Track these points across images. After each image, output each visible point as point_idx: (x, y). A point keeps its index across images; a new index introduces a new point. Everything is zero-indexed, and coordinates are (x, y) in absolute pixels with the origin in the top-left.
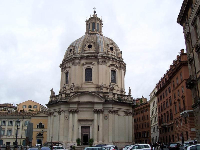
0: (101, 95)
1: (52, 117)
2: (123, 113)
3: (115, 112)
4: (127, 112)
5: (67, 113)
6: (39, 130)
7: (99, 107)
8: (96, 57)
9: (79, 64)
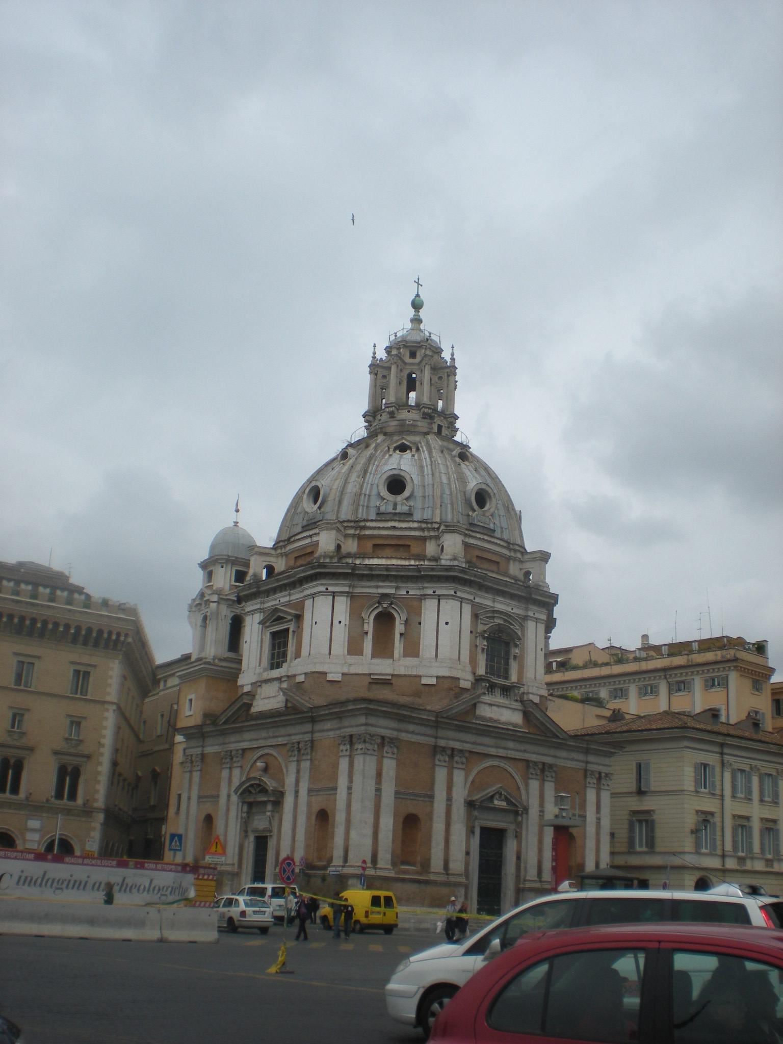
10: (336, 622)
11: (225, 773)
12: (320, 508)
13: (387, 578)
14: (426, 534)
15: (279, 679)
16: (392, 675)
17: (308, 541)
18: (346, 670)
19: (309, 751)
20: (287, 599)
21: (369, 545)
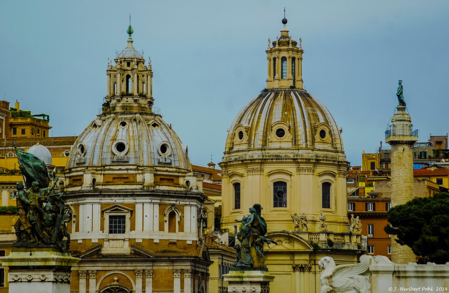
0: (306, 237)
7: (301, 260)
8: (295, 161)
9: (261, 170)
10: (155, 216)
11: (82, 281)
12: (126, 155)
13: (173, 197)
14: (180, 174)
15: (124, 240)
16: (177, 240)
17: (125, 172)
18: (160, 239)
19: (151, 274)
20: (122, 201)
21: (158, 178)
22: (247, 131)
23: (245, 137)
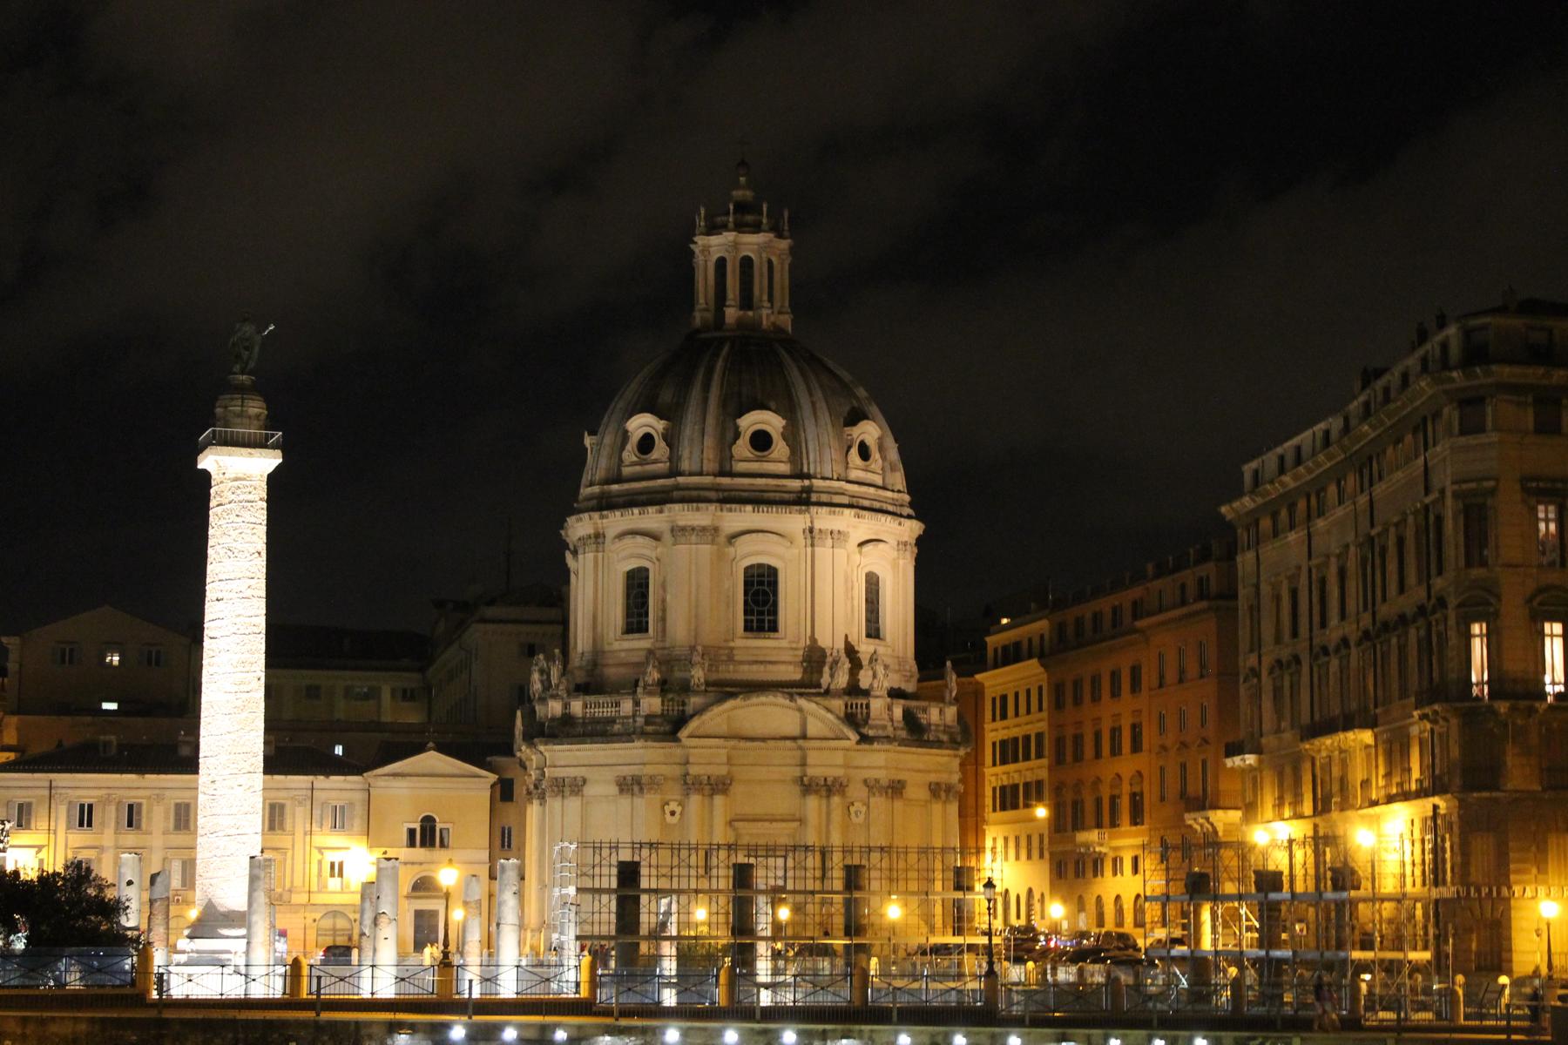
1: (573, 804)
2: (924, 794)
3: (896, 789)
4: (938, 784)
5: (674, 792)
6: (419, 853)
7: (824, 763)
22: (665, 437)
23: (660, 450)
